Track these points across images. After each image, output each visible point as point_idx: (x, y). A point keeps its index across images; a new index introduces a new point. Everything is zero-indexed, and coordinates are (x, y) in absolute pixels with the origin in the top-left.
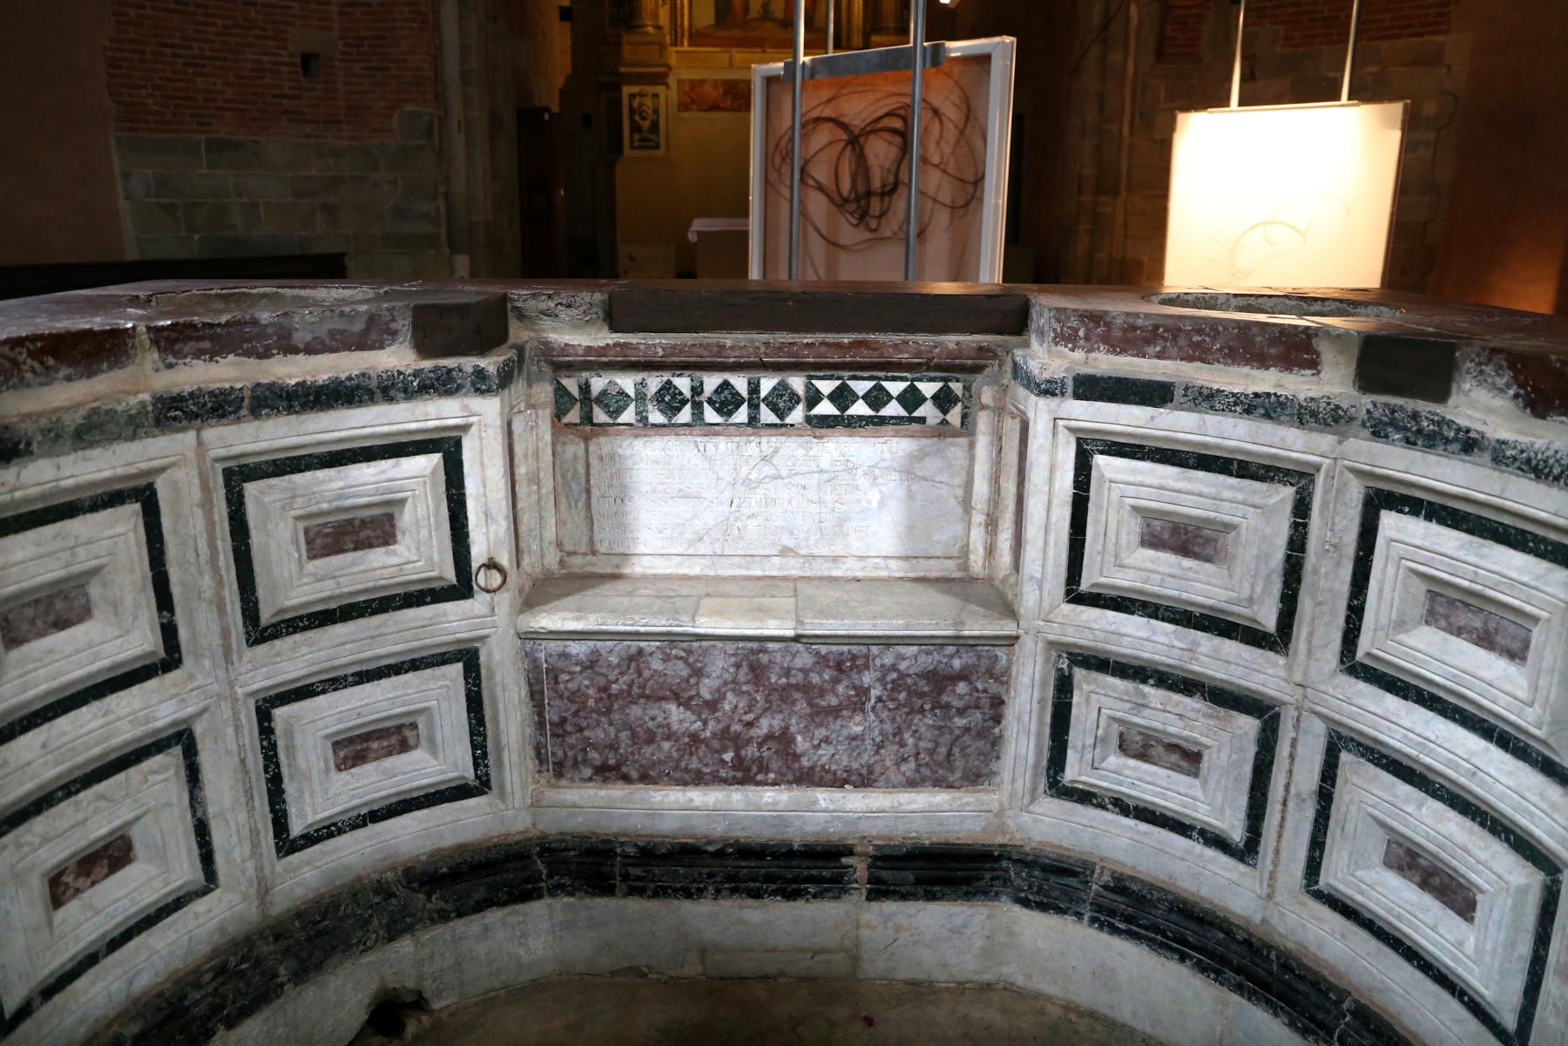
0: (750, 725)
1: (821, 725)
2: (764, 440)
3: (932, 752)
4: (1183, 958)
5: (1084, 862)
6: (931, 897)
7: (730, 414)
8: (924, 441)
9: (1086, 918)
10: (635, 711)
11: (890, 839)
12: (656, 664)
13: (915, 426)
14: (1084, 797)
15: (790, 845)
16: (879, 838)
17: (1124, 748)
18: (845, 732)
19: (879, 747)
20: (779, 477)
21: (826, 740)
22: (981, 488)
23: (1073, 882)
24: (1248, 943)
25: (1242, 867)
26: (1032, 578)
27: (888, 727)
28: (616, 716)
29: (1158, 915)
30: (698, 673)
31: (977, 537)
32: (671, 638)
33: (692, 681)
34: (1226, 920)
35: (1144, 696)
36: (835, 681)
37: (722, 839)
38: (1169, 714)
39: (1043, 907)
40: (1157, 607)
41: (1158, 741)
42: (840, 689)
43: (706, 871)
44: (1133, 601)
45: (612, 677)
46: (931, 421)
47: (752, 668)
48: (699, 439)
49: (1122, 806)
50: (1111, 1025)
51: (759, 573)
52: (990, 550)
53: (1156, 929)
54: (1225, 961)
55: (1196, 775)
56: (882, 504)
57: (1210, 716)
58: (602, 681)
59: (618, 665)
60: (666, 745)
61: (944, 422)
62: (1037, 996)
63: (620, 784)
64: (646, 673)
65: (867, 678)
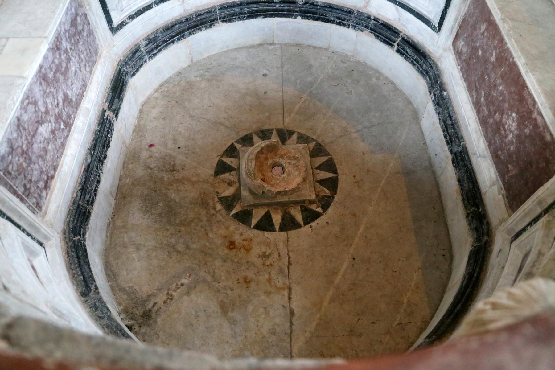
4: (173, 42)
5: (136, 45)
9: (147, 60)
10: (35, 146)
11: (105, 96)
14: (122, 25)
15: (96, 130)
16: (103, 100)
18: (73, 74)
21: (72, 84)
23: (138, 54)
24: (187, 20)
27: (77, 58)
28: (34, 158)
29: (161, 39)
30: (35, 103)
33: (37, 109)
37: (87, 154)
39: (137, 70)
42: (63, 57)
43: (95, 169)
45: (20, 144)
47: (44, 79)
49: (131, 18)
50: (167, 82)
53: (164, 42)
54: (183, 31)
58: (19, 150)
59: (18, 136)
60: (50, 147)
62: (149, 98)
63: (53, 182)
64: (26, 126)
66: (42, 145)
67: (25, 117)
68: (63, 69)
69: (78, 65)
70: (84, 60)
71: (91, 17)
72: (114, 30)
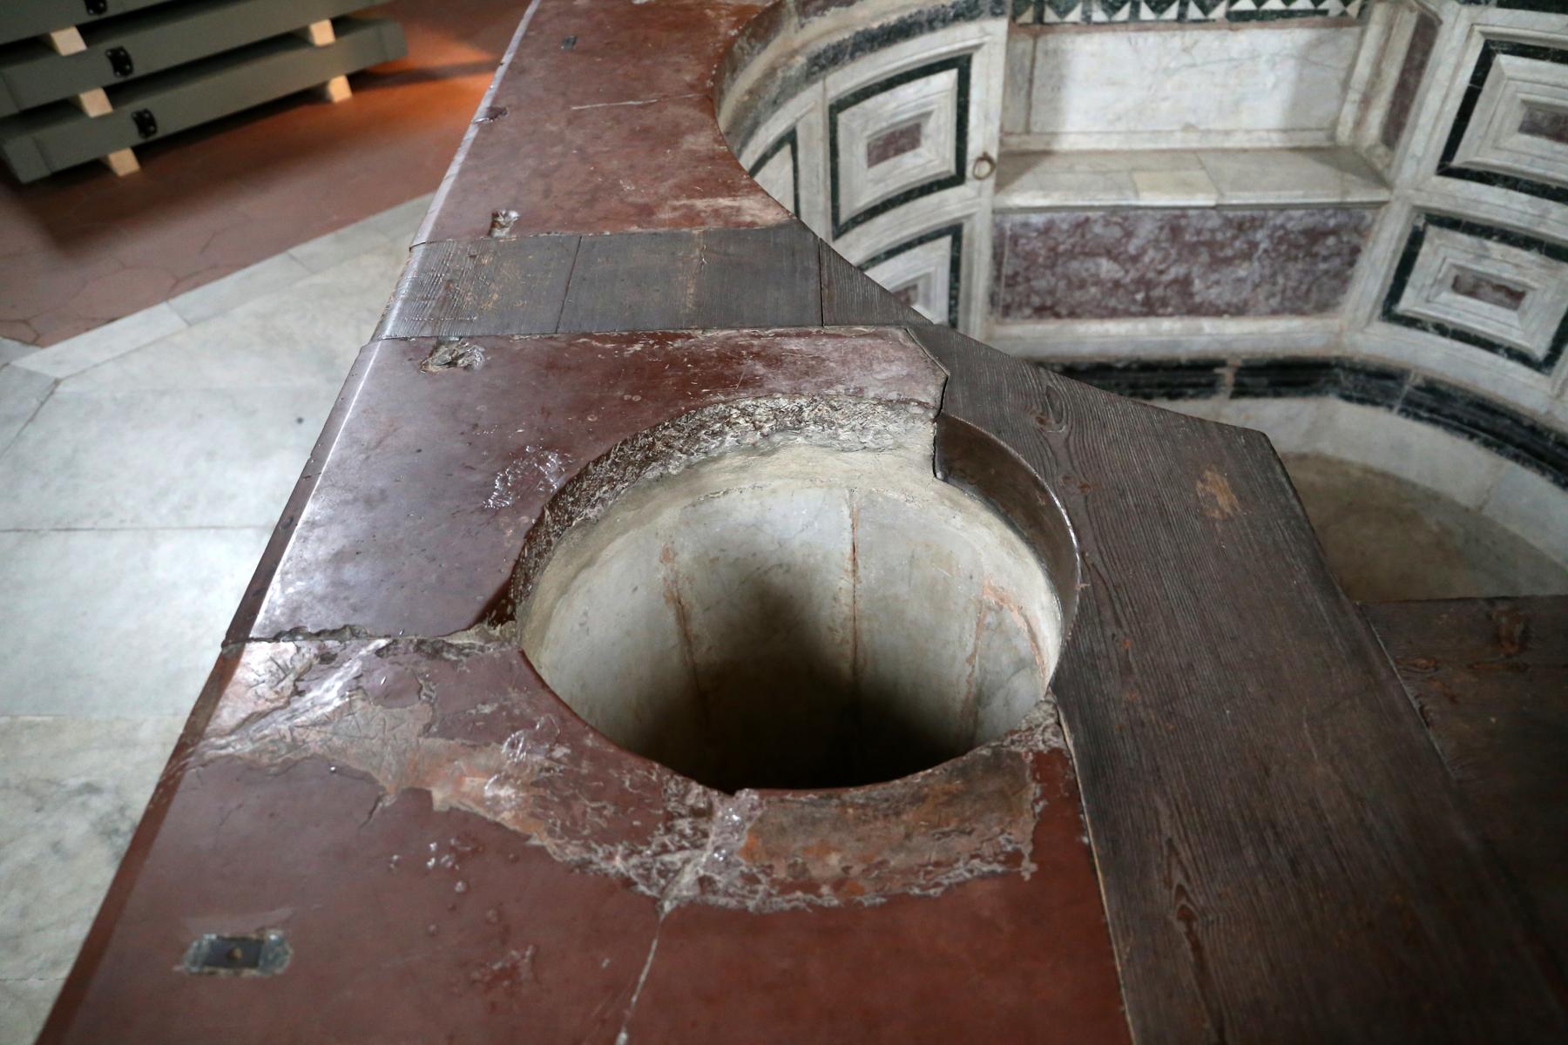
0: (1161, 272)
1: (1214, 271)
2: (1188, 34)
3: (1295, 289)
4: (1472, 437)
6: (1277, 395)
7: (1162, 11)
8: (1324, 31)
10: (1074, 265)
12: (1098, 229)
13: (1318, 18)
14: (1411, 322)
17: (1457, 286)
19: (1256, 286)
20: (1194, 65)
21: (1217, 283)
22: (1363, 70)
23: (1390, 384)
25: (1537, 375)
26: (1414, 156)
27: (1267, 272)
28: (1059, 270)
29: (1458, 408)
30: (1129, 234)
31: (1349, 113)
32: (1114, 210)
34: (1515, 412)
35: (1486, 249)
36: (1235, 238)
38: (1503, 262)
39: (1361, 401)
40: (1517, 181)
41: (1489, 283)
42: (1237, 244)
44: (1496, 176)
46: (1333, 13)
48: (1133, 35)
49: (1442, 329)
50: (1399, 482)
51: (1164, 146)
52: (1359, 123)
53: (1454, 417)
55: (1515, 308)
56: (1275, 86)
57: (1543, 266)
58: (1051, 243)
60: (1093, 290)
61: (1344, 14)
62: (1341, 462)
63: (1052, 320)
64: (1088, 236)
65: (1260, 235)
66: (1084, 274)
67: (1098, 229)
68: (1221, 255)
69: (1257, 279)
70: (1278, 288)
71: (1363, 261)
72: (1389, 312)
